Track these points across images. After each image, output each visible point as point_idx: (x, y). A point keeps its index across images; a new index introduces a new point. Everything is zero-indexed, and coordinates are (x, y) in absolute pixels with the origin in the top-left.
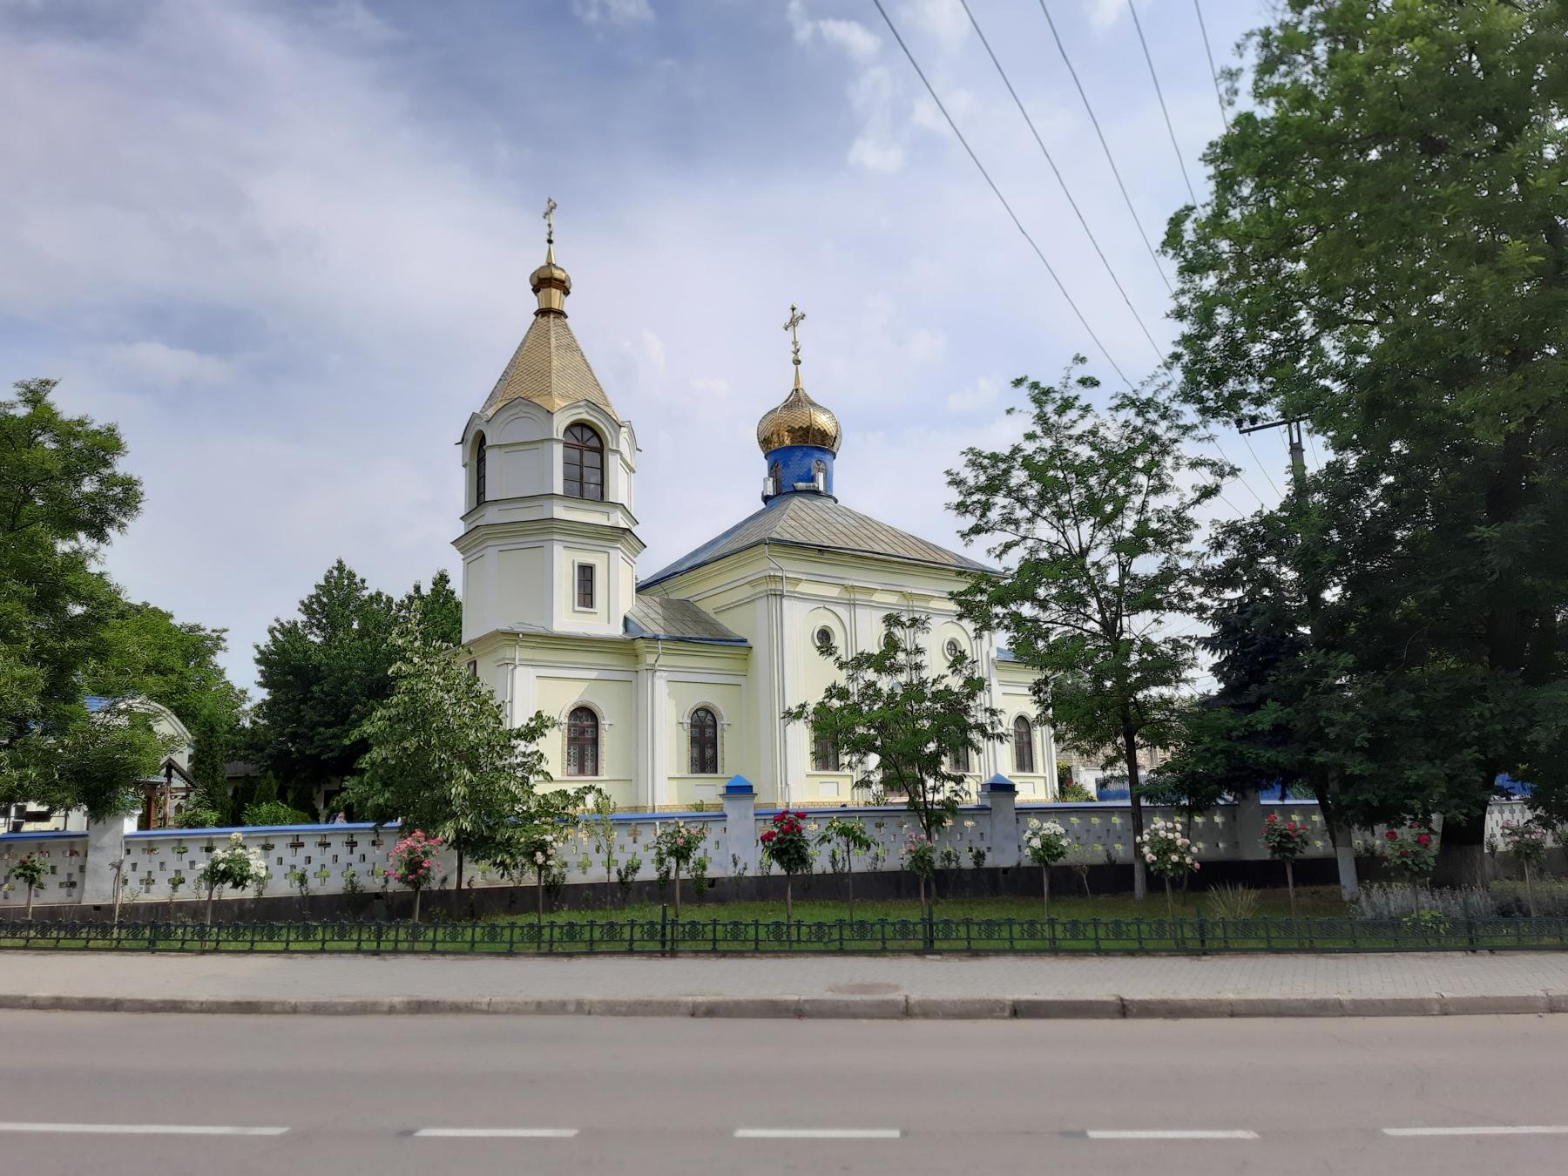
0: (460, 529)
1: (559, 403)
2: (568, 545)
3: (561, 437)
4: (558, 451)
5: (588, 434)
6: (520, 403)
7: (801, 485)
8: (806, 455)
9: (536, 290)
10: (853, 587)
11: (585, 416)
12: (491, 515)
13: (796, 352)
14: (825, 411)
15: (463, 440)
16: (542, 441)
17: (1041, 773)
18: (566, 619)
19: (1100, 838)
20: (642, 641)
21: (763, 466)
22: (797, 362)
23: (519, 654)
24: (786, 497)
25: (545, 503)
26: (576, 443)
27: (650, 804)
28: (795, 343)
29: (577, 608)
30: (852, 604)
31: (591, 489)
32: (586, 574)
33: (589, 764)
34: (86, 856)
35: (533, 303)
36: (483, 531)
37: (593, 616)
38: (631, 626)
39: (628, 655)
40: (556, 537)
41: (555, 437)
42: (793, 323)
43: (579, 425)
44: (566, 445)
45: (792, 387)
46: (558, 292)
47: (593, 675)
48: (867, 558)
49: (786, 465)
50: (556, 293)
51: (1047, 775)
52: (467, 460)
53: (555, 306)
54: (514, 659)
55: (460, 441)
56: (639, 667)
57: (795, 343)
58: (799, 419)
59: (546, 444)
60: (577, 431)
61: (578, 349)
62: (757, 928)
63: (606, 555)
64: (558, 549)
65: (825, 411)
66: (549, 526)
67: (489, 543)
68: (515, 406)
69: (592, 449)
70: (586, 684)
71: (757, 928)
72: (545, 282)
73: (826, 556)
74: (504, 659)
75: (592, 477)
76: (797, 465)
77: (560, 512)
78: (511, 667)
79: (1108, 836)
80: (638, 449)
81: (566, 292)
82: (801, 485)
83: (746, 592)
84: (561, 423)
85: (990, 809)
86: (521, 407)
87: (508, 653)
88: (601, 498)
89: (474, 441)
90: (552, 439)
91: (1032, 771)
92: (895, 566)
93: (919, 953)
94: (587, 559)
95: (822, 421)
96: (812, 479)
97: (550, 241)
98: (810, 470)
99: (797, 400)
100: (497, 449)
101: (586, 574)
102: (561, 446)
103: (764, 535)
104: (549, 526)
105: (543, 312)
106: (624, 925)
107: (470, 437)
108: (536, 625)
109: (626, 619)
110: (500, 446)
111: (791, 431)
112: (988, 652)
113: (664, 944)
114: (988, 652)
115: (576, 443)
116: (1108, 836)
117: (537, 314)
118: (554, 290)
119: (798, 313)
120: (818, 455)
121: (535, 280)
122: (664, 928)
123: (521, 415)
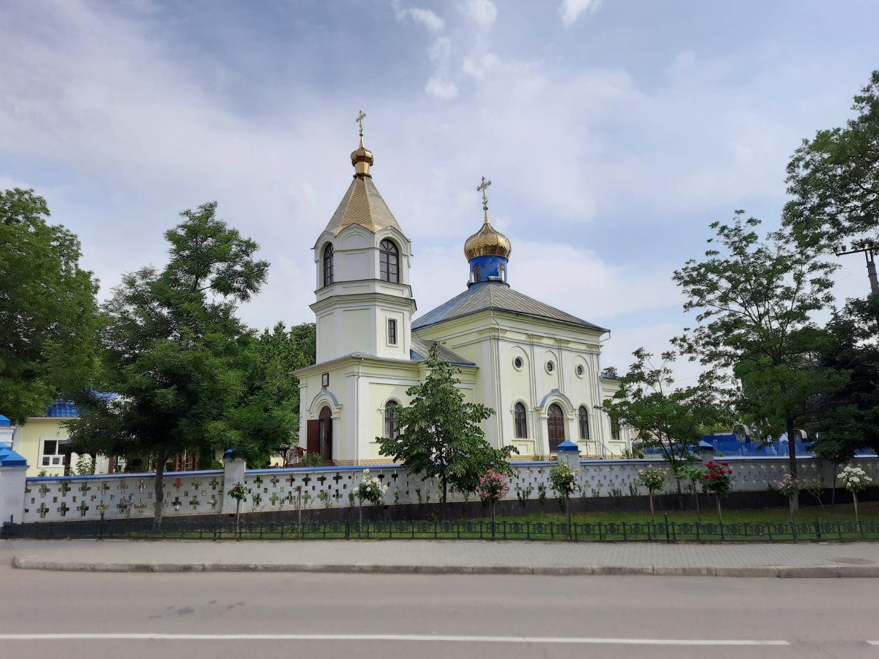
0: (314, 299)
1: (377, 228)
2: (383, 308)
3: (378, 247)
4: (377, 253)
5: (390, 246)
6: (355, 227)
7: (492, 278)
8: (494, 261)
9: (354, 163)
10: (532, 335)
11: (390, 235)
12: (338, 290)
13: (485, 203)
14: (503, 236)
15: (315, 246)
16: (368, 249)
17: (623, 440)
18: (384, 351)
19: (776, 476)
21: (467, 266)
23: (362, 370)
24: (483, 284)
25: (371, 284)
26: (385, 250)
28: (484, 198)
29: (389, 344)
30: (532, 345)
31: (393, 278)
32: (393, 323)
33: (617, 437)
34: (223, 485)
35: (353, 171)
37: (396, 348)
38: (414, 354)
39: (414, 371)
40: (377, 303)
41: (376, 246)
43: (387, 240)
44: (381, 252)
45: (483, 222)
46: (367, 164)
47: (397, 382)
48: (539, 319)
49: (483, 266)
50: (366, 165)
51: (626, 441)
52: (318, 258)
53: (366, 172)
54: (358, 373)
55: (313, 247)
57: (484, 198)
58: (490, 241)
59: (371, 251)
60: (385, 243)
61: (379, 197)
62: (552, 526)
63: (402, 314)
64: (378, 310)
65: (503, 236)
66: (374, 297)
67: (338, 306)
68: (352, 228)
69: (393, 254)
70: (393, 388)
71: (552, 526)
72: (360, 158)
73: (520, 317)
74: (353, 372)
75: (393, 269)
76: (489, 266)
77: (379, 289)
78: (356, 377)
79: (760, 475)
80: (411, 255)
81: (371, 164)
82: (492, 278)
83: (475, 337)
84: (378, 238)
85: (701, 460)
86: (355, 229)
87: (355, 369)
88: (398, 282)
89: (322, 248)
90: (374, 248)
91: (619, 439)
92: (553, 324)
93: (813, 541)
94: (393, 316)
95: (502, 241)
96: (497, 274)
97: (361, 135)
98: (496, 269)
99: (486, 230)
101: (393, 323)
102: (379, 251)
103: (488, 305)
104: (374, 297)
106: (595, 526)
107: (321, 245)
108: (365, 352)
109: (411, 350)
110: (343, 251)
111: (486, 247)
112: (597, 373)
113: (668, 536)
114: (597, 373)
115: (385, 250)
116: (760, 475)
117: (355, 177)
118: (365, 163)
119: (486, 181)
120: (500, 260)
121: (355, 157)
122: (667, 527)
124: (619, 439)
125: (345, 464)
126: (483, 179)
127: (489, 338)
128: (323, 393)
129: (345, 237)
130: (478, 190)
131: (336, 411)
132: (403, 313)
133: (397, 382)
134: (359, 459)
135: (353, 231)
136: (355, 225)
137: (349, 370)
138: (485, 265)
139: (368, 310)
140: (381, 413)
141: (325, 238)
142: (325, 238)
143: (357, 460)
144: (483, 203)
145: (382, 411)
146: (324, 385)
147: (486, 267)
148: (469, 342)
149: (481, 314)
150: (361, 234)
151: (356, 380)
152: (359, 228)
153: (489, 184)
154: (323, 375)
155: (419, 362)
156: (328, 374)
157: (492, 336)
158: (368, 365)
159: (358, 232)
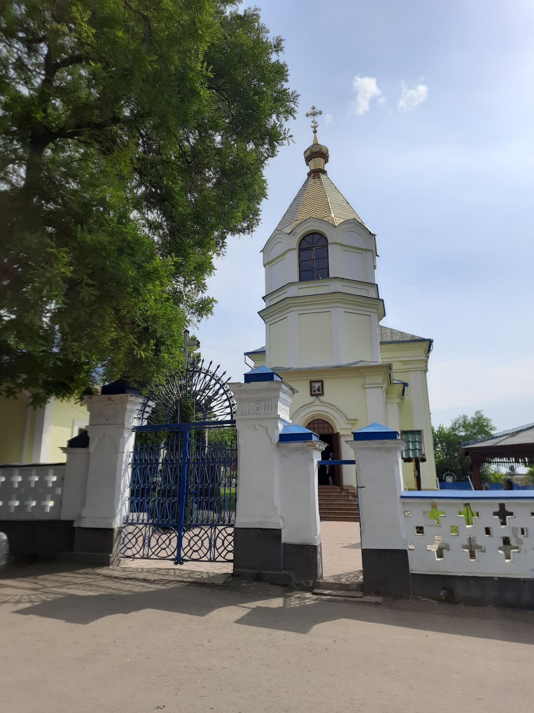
15: (291, 232)
16: (366, 250)
67: (338, 305)
86: (353, 225)
110: (341, 245)
123: (353, 229)
127: (421, 369)
128: (317, 403)
136: (354, 220)
139: (368, 317)
141: (311, 225)
146: (313, 393)
148: (409, 368)
149: (401, 345)
150: (361, 234)
152: (357, 225)
154: (311, 382)
156: (322, 382)
159: (356, 229)
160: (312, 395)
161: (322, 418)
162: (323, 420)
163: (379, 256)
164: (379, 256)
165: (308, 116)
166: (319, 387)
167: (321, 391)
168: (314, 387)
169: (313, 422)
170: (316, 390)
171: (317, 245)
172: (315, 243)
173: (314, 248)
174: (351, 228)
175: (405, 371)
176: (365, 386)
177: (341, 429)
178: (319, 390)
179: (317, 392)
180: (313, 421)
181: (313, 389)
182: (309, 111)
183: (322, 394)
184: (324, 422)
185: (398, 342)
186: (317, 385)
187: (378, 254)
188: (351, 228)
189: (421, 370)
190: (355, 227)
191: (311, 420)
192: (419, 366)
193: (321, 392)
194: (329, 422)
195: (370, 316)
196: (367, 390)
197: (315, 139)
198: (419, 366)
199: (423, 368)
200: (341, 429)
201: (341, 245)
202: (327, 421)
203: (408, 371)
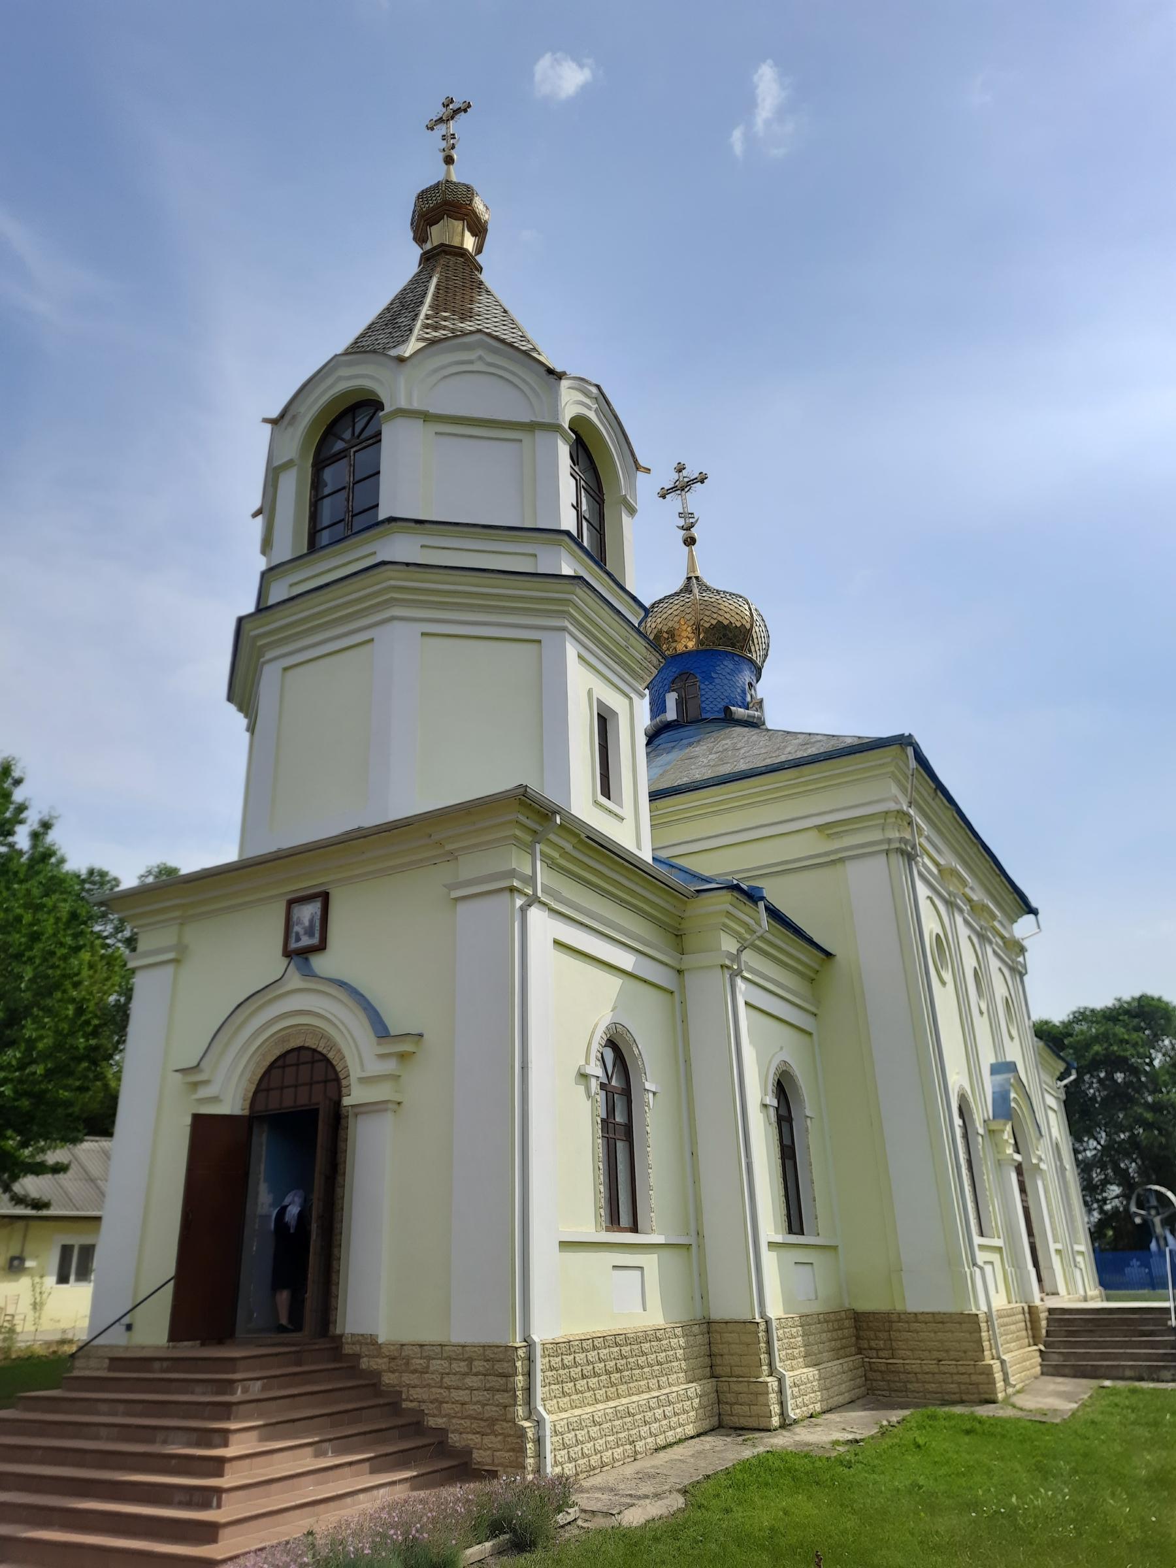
15: (283, 415)
16: (532, 427)
20: (727, 897)
22: (690, 541)
24: (711, 727)
27: (984, 1308)
36: (392, 578)
42: (682, 487)
47: (626, 961)
55: (274, 414)
56: (689, 961)
59: (540, 436)
68: (468, 347)
70: (615, 983)
74: (512, 874)
83: (812, 845)
86: (480, 352)
100: (418, 424)
105: (428, 259)
107: (308, 412)
110: (426, 417)
119: (691, 472)
123: (478, 366)
124: (634, 1229)
125: (436, 1365)
126: (680, 469)
127: (885, 847)
128: (295, 980)
129: (435, 371)
130: (664, 497)
131: (375, 1067)
132: (631, 699)
133: (626, 961)
134: (535, 1338)
135: (473, 355)
136: (478, 336)
137: (473, 866)
138: (714, 675)
139: (534, 646)
140: (589, 1096)
142: (340, 379)
143: (529, 1344)
144: (682, 528)
145: (594, 1085)
146: (293, 945)
147: (717, 681)
151: (517, 915)
152: (495, 351)
153: (702, 482)
154: (291, 903)
155: (698, 891)
157: (901, 840)
158: (556, 855)
160: (288, 953)
161: (311, 1043)
162: (314, 1050)
163: (648, 470)
164: (648, 470)
165: (432, 129)
166: (311, 921)
167: (317, 935)
168: (299, 922)
169: (280, 1063)
170: (301, 932)
171: (362, 437)
172: (357, 433)
173: (355, 449)
174: (471, 362)
175: (833, 862)
176: (456, 894)
177: (364, 1081)
178: (310, 932)
179: (306, 941)
180: (283, 1056)
181: (297, 928)
182: (439, 111)
183: (321, 947)
184: (317, 1057)
185: (797, 764)
186: (308, 913)
187: (642, 462)
188: (471, 362)
189: (887, 852)
190: (490, 358)
191: (277, 1052)
192: (876, 835)
193: (315, 941)
194: (330, 1056)
195: (539, 641)
196: (462, 907)
197: (448, 172)
198: (876, 835)
199: (889, 841)
200: (364, 1081)
201: (426, 417)
202: (325, 1052)
203: (842, 860)
